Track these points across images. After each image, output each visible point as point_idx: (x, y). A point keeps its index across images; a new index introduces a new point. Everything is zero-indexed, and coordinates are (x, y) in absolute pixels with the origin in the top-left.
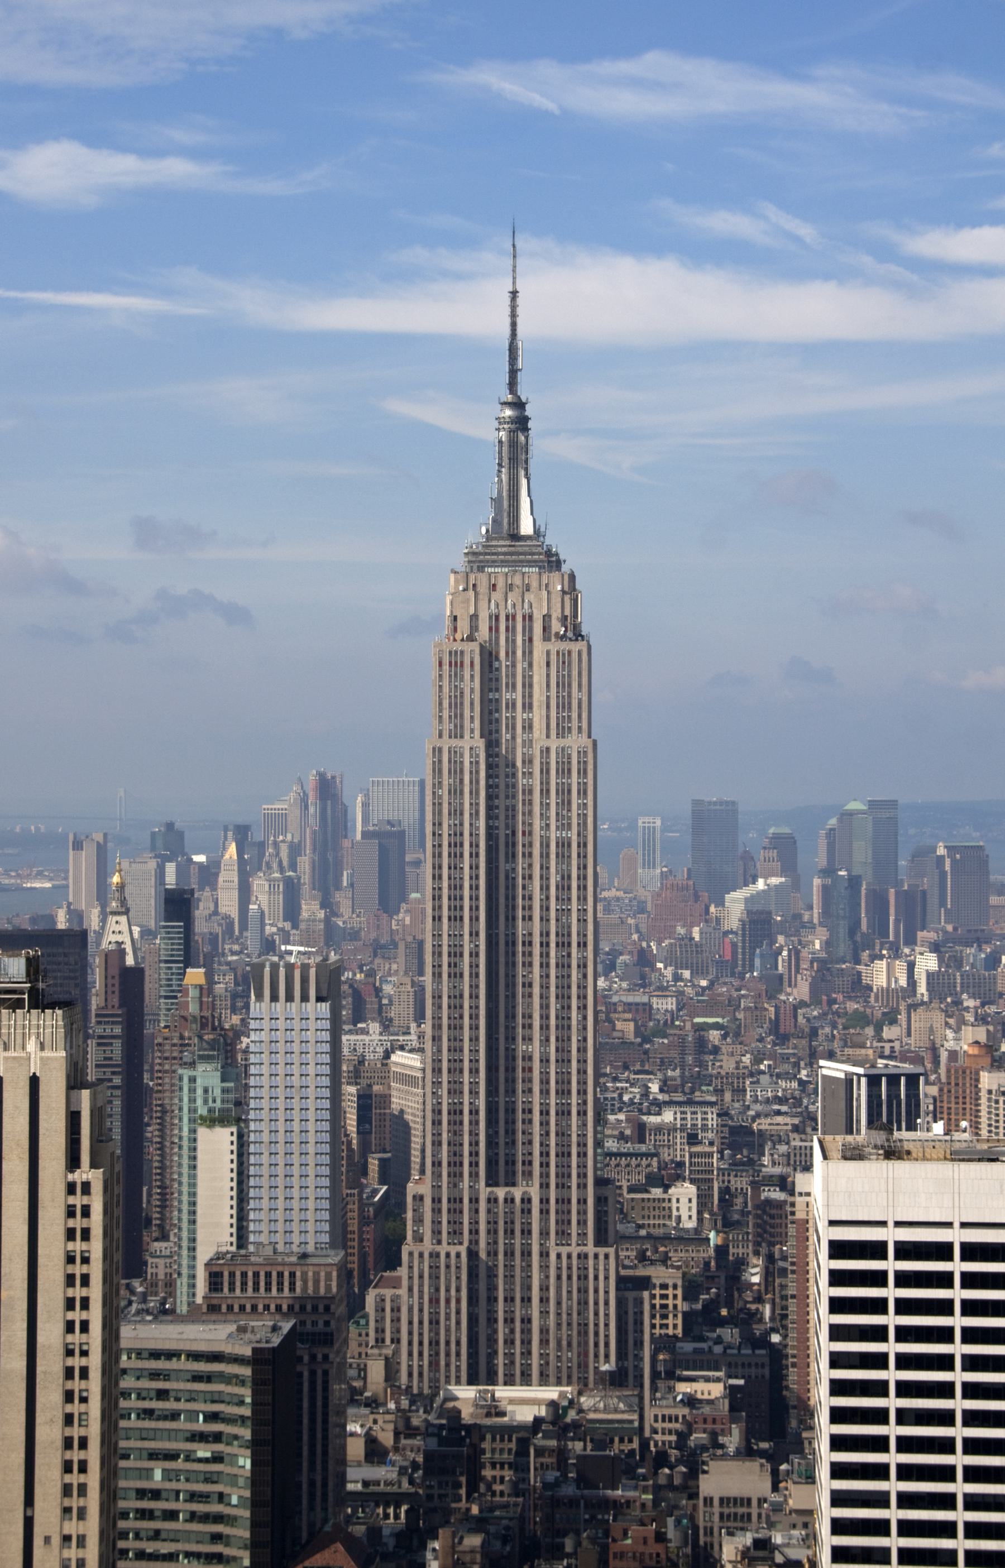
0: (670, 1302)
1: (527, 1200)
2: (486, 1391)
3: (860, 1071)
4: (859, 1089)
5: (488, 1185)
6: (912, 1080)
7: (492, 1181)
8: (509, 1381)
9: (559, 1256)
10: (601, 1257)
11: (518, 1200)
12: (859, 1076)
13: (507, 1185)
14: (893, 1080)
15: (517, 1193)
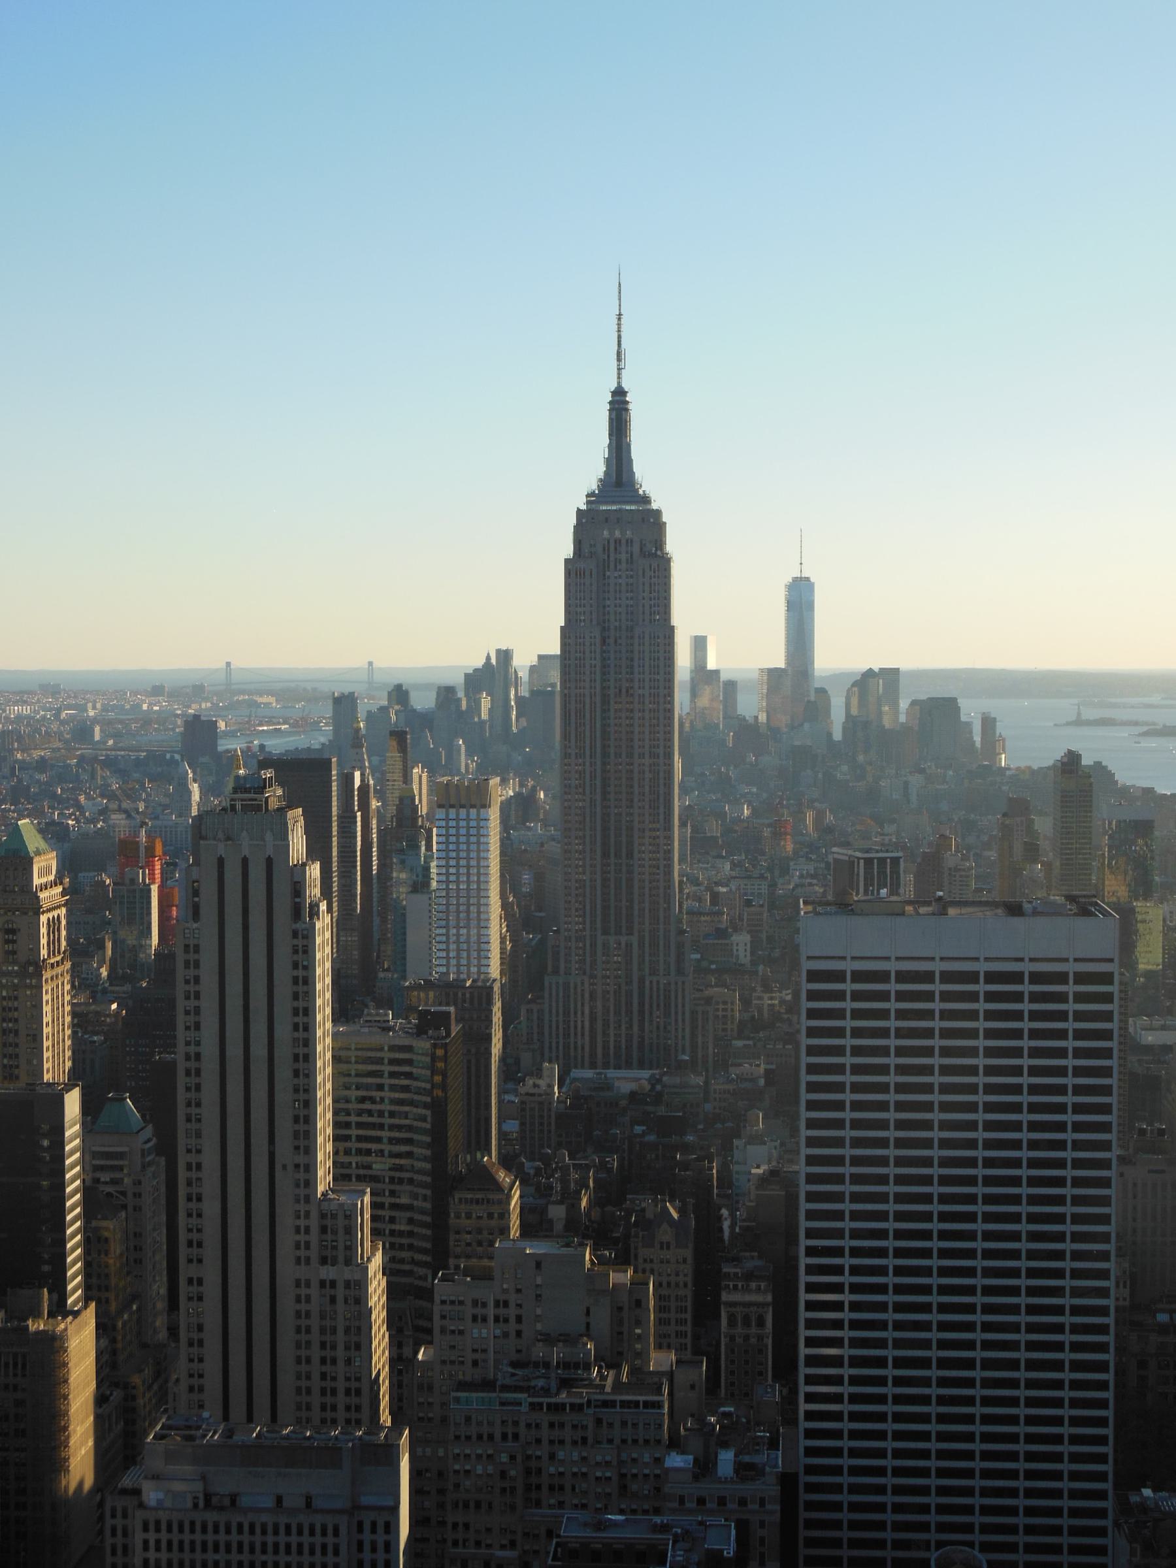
0: (729, 1014)
1: (629, 946)
2: (600, 1074)
3: (858, 854)
4: (858, 868)
5: (602, 934)
6: (895, 861)
7: (606, 932)
8: (618, 1067)
9: (651, 982)
10: (680, 983)
11: (623, 945)
12: (859, 859)
13: (616, 934)
14: (882, 861)
15: (623, 939)
